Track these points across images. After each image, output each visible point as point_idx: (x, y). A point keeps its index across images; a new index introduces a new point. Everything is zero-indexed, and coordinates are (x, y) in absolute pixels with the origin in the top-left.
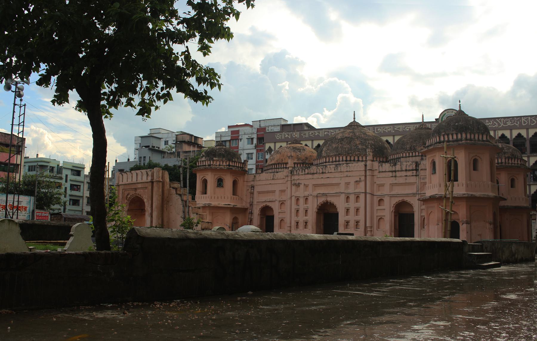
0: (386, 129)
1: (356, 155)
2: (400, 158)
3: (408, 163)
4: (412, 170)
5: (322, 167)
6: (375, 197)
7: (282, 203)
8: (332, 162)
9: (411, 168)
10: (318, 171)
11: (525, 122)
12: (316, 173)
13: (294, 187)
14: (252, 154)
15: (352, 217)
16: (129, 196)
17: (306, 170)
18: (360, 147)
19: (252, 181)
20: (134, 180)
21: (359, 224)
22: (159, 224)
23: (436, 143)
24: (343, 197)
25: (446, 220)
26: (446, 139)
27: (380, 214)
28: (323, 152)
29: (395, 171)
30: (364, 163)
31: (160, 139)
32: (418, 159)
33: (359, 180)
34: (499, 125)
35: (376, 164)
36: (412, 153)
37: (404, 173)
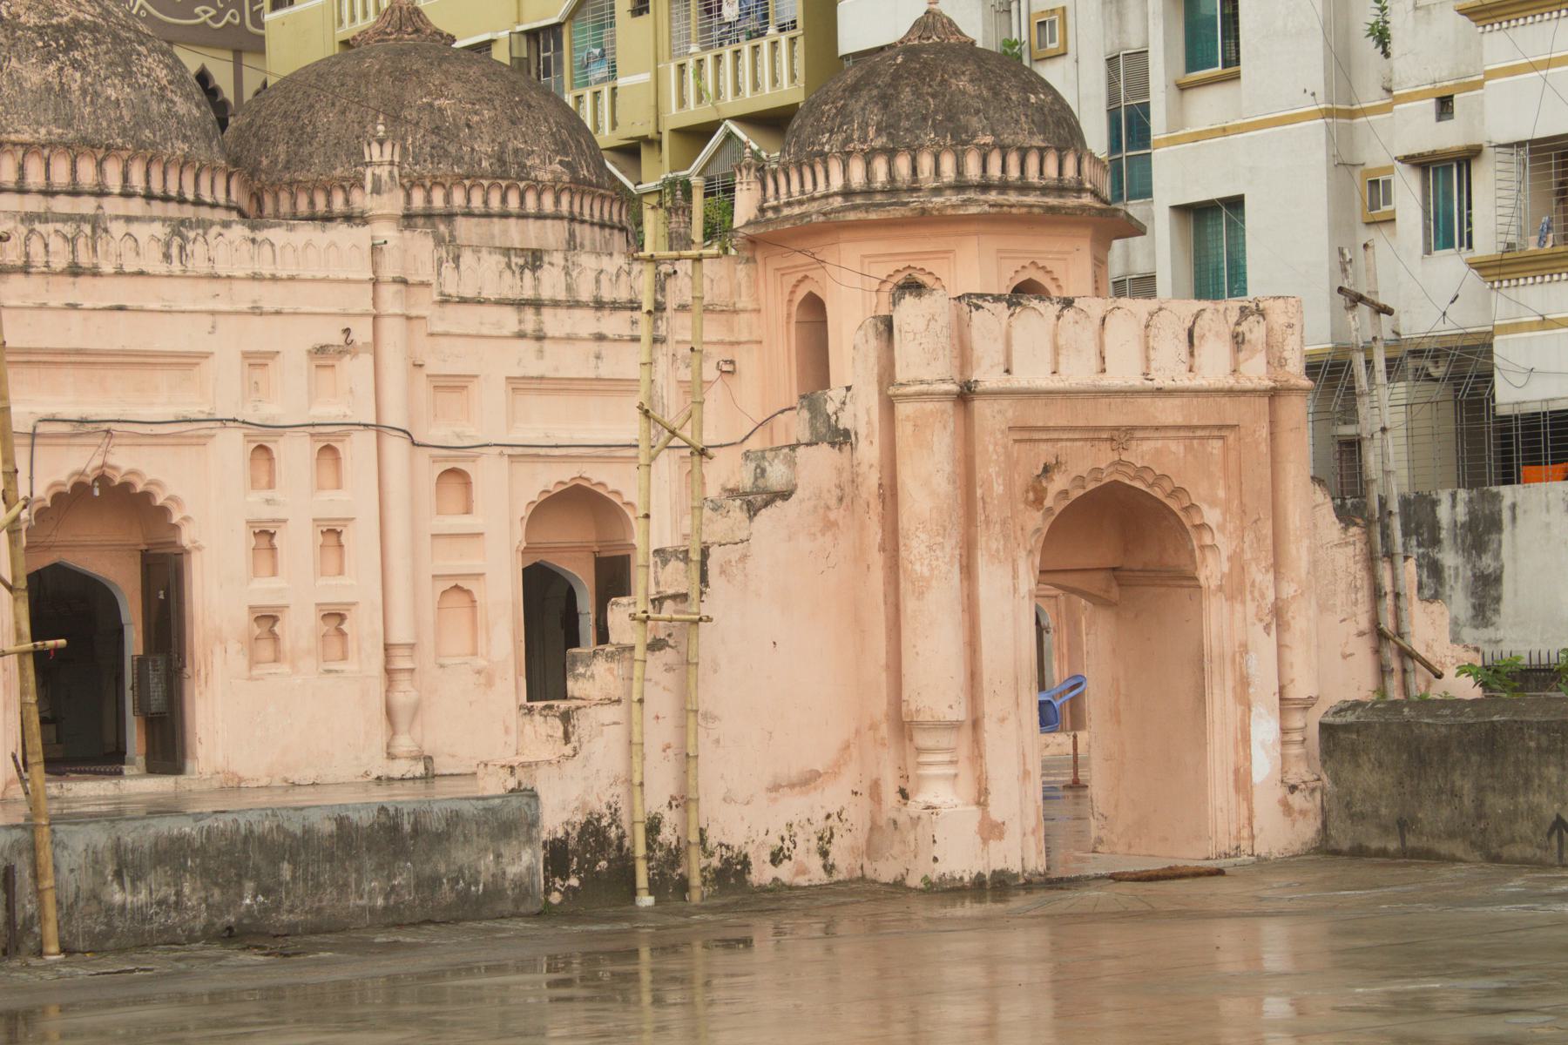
2: (449, 216)
4: (634, 306)
5: (68, 229)
8: (48, 192)
9: (623, 295)
10: (38, 258)
12: (25, 270)
15: (298, 586)
16: (1058, 483)
20: (1125, 374)
24: (232, 447)
26: (1014, 173)
27: (457, 562)
29: (537, 304)
33: (337, 339)
35: (421, 245)
37: (585, 323)
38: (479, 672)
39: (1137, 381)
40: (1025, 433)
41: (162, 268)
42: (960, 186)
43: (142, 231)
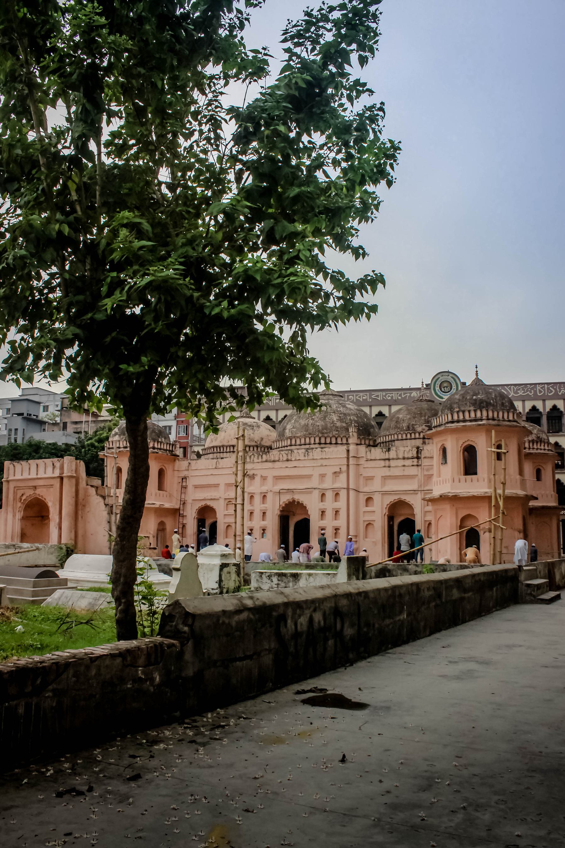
0: (360, 397)
1: (334, 436)
3: (407, 449)
4: (413, 458)
5: (286, 452)
6: (361, 495)
9: (410, 455)
11: (540, 392)
14: (170, 427)
15: (329, 523)
16: (24, 498)
17: (264, 456)
18: (338, 424)
19: (186, 470)
20: (33, 475)
21: (339, 531)
22: (71, 539)
23: (448, 423)
24: (316, 495)
25: (461, 527)
26: (461, 417)
27: (368, 518)
28: (287, 431)
29: (389, 459)
30: (345, 447)
31: (39, 403)
32: (419, 443)
33: (338, 470)
35: (362, 448)
36: (411, 434)
37: (401, 462)
38: (373, 542)
39: (35, 476)
41: (303, 458)
42: (448, 423)
43: (300, 451)
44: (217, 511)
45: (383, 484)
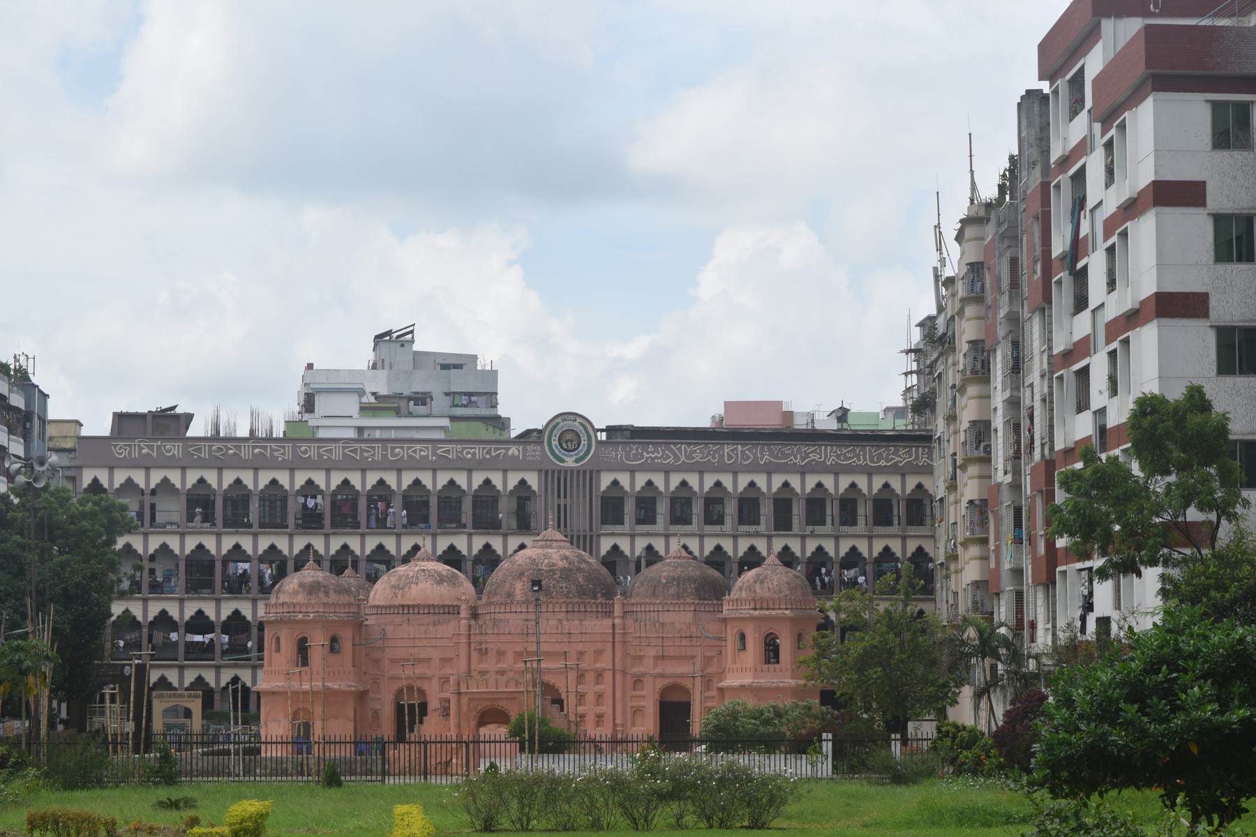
7: (445, 680)
11: (730, 457)
13: (475, 655)
24: (572, 676)
28: (518, 592)
30: (609, 622)
34: (677, 458)
40: (471, 700)
44: (427, 692)
45: (655, 666)
